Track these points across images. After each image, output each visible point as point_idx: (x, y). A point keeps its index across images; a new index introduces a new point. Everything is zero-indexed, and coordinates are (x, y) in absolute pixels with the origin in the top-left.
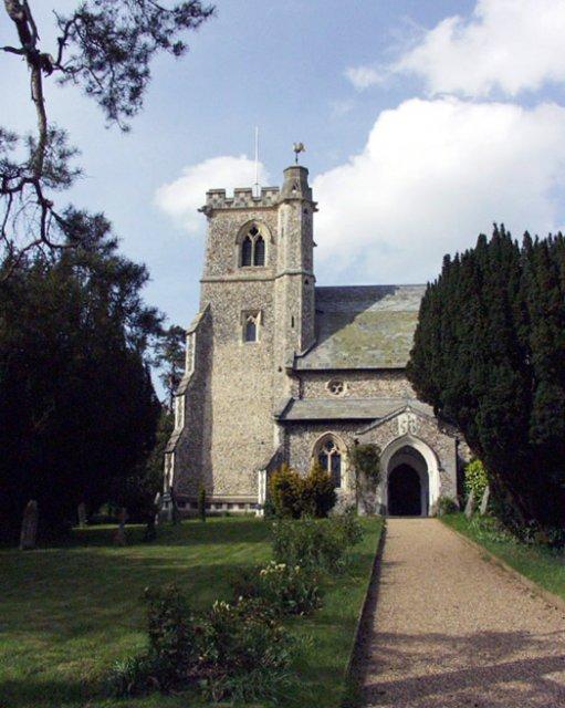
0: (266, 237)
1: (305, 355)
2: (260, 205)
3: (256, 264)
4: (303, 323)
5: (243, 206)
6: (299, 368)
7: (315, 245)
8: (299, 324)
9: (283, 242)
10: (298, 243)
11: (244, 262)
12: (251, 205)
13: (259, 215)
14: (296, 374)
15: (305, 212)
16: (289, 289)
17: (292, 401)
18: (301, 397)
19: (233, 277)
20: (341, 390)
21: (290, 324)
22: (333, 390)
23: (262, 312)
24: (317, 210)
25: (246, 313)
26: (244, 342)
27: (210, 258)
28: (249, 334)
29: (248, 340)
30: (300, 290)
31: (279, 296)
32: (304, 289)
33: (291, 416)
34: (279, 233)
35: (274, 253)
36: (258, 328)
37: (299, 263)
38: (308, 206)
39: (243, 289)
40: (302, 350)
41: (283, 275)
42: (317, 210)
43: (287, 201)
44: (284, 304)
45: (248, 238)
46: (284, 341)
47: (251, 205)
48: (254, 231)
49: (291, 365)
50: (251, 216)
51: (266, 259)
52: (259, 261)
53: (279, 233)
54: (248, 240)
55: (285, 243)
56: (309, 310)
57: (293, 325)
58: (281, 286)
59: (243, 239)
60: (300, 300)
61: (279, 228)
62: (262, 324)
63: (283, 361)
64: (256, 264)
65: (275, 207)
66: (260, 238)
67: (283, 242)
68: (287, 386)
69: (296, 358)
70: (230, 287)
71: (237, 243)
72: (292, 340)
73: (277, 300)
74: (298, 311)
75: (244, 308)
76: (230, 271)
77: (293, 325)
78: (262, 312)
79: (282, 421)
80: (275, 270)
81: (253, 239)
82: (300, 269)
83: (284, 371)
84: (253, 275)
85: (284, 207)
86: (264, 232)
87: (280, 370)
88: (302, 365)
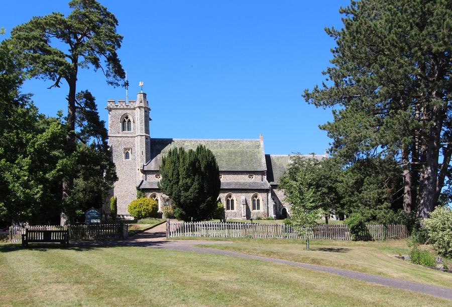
0: (132, 120)
3: (128, 130)
4: (146, 154)
5: (122, 107)
7: (151, 120)
8: (144, 154)
9: (138, 122)
10: (144, 124)
11: (123, 130)
12: (125, 107)
13: (128, 111)
14: (144, 172)
15: (145, 111)
16: (141, 141)
17: (143, 181)
18: (146, 180)
20: (159, 177)
25: (125, 149)
28: (127, 156)
29: (126, 159)
32: (146, 141)
33: (142, 187)
37: (144, 131)
39: (124, 140)
43: (140, 107)
44: (139, 147)
45: (125, 120)
46: (140, 160)
48: (127, 118)
49: (142, 169)
50: (125, 111)
51: (132, 129)
52: (129, 129)
53: (136, 119)
54: (125, 121)
58: (138, 139)
59: (122, 121)
60: (144, 145)
61: (136, 117)
63: (139, 167)
64: (128, 130)
65: (134, 109)
66: (129, 120)
67: (138, 122)
68: (141, 176)
69: (144, 166)
70: (119, 139)
72: (142, 160)
73: (136, 144)
74: (144, 150)
76: (119, 133)
79: (138, 188)
80: (135, 134)
81: (126, 120)
82: (144, 134)
84: (128, 135)
86: (130, 118)
88: (146, 169)
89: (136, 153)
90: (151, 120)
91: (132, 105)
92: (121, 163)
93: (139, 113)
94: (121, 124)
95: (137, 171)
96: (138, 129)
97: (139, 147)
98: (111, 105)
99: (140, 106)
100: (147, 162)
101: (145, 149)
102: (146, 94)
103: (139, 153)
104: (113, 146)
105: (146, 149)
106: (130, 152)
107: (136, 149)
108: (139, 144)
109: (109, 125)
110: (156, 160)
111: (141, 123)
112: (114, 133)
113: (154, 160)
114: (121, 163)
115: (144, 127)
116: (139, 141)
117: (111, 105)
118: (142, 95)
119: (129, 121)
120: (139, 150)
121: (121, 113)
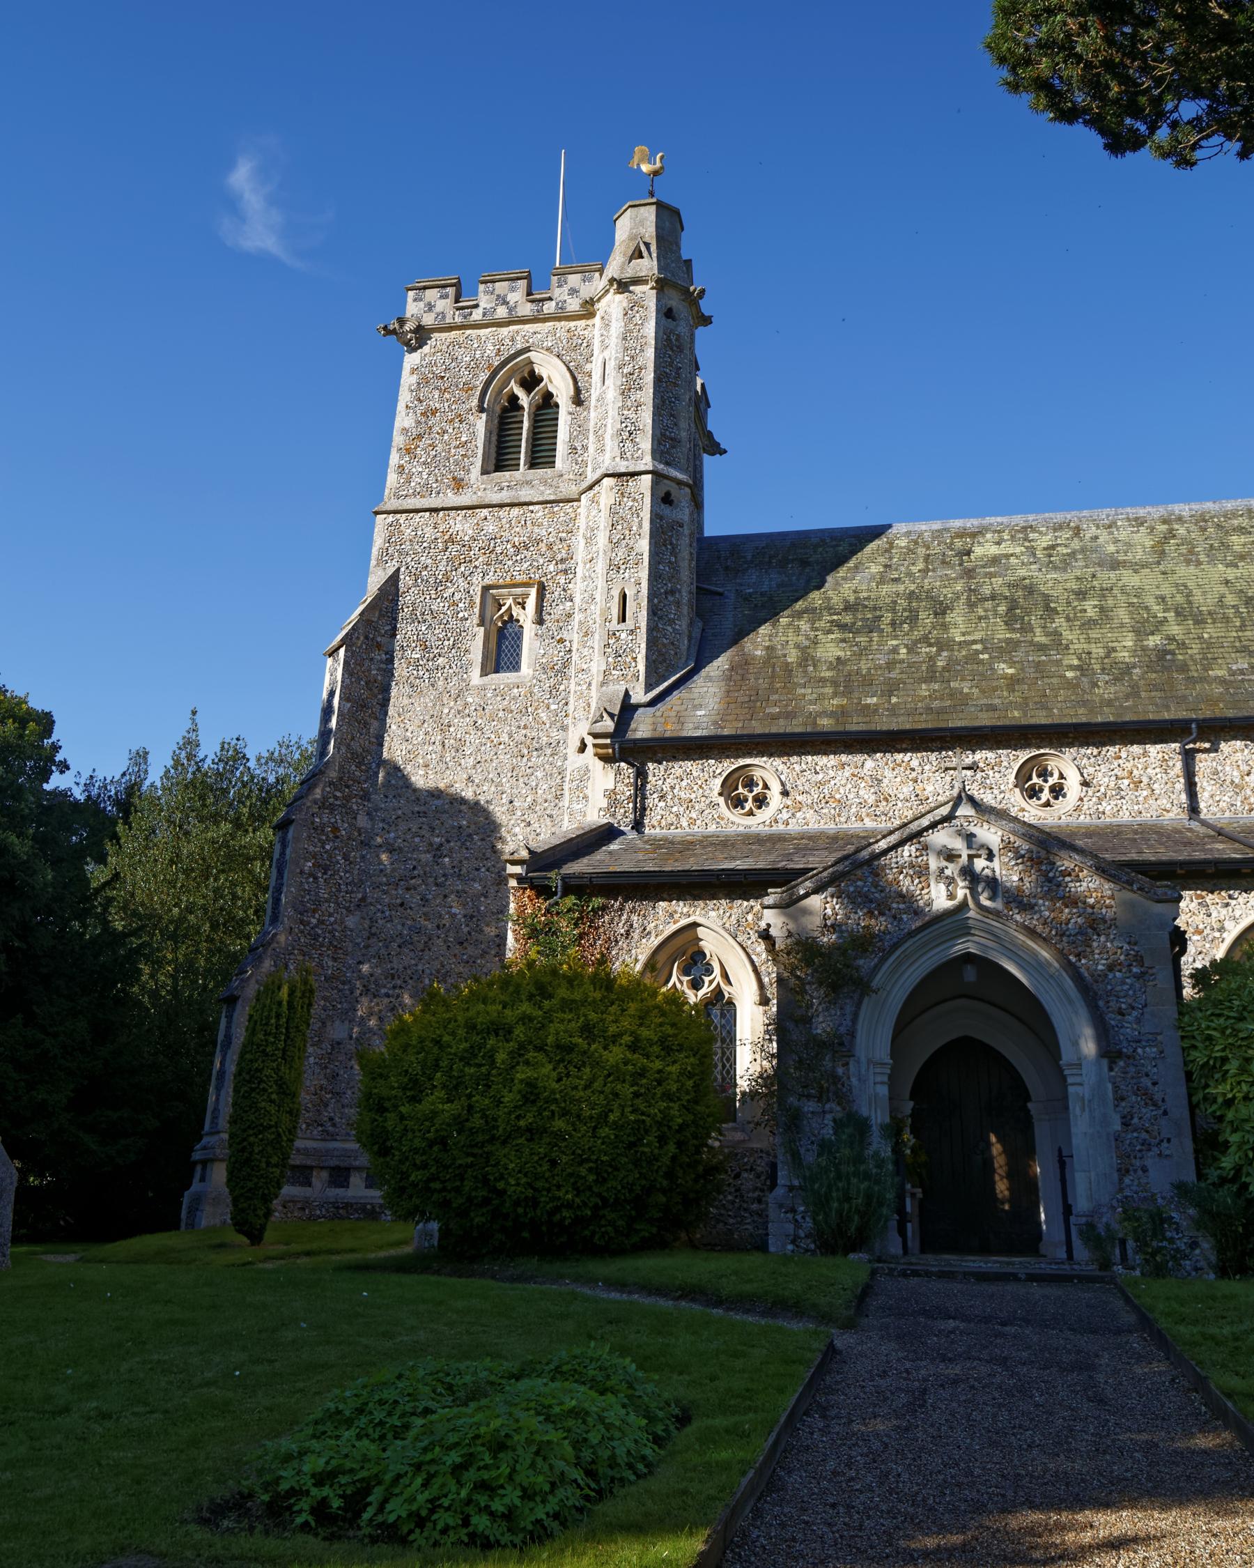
0: (561, 389)
1: (652, 703)
2: (549, 307)
4: (653, 611)
5: (502, 312)
6: (630, 735)
7: (716, 449)
8: (639, 614)
10: (647, 395)
19: (465, 499)
20: (761, 801)
21: (615, 611)
22: (738, 802)
23: (542, 589)
24: (706, 321)
26: (484, 673)
27: (408, 451)
30: (646, 515)
31: (589, 540)
32: (656, 517)
34: (596, 377)
35: (580, 429)
36: (529, 629)
37: (646, 444)
38: (675, 301)
39: (490, 528)
40: (649, 687)
41: (598, 482)
42: (706, 321)
43: (623, 286)
45: (514, 399)
46: (597, 665)
47: (526, 309)
48: (531, 381)
52: (541, 456)
53: (596, 377)
55: (612, 394)
56: (674, 567)
57: (623, 619)
60: (644, 545)
61: (595, 368)
62: (540, 621)
64: (533, 465)
66: (548, 396)
70: (461, 526)
71: (481, 409)
73: (580, 554)
74: (638, 581)
75: (487, 581)
76: (459, 484)
77: (623, 619)
78: (542, 589)
81: (524, 400)
82: (647, 462)
83: (590, 750)
84: (525, 494)
85: (613, 304)
86: (558, 382)
87: (583, 748)
88: (642, 728)
89: (578, 617)
90: (716, 449)
91: (573, 292)
92: (449, 708)
93: (617, 327)
94: (480, 424)
95: (575, 761)
96: (600, 439)
97: (601, 566)
98: (430, 307)
99: (629, 273)
100: (653, 676)
101: (644, 574)
102: (675, 213)
103: (596, 610)
104: (405, 580)
105: (655, 576)
106: (526, 617)
107: (577, 588)
108: (602, 539)
109: (398, 440)
110: (740, 670)
111: (625, 393)
112: (427, 490)
113: (720, 665)
114: (449, 708)
115: (646, 417)
116: (603, 520)
117: (430, 307)
118: (654, 207)
119: (547, 403)
120: (601, 583)
121: (490, 350)
